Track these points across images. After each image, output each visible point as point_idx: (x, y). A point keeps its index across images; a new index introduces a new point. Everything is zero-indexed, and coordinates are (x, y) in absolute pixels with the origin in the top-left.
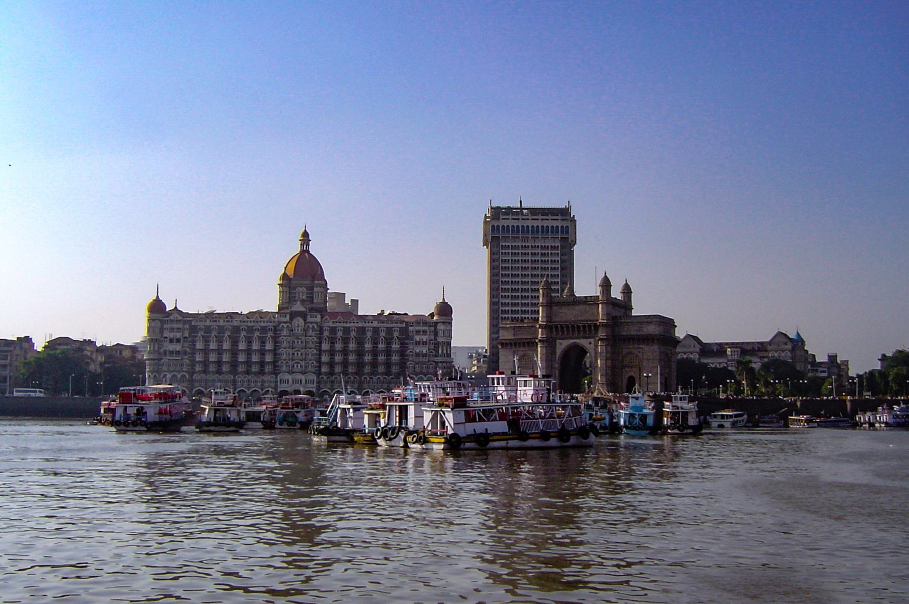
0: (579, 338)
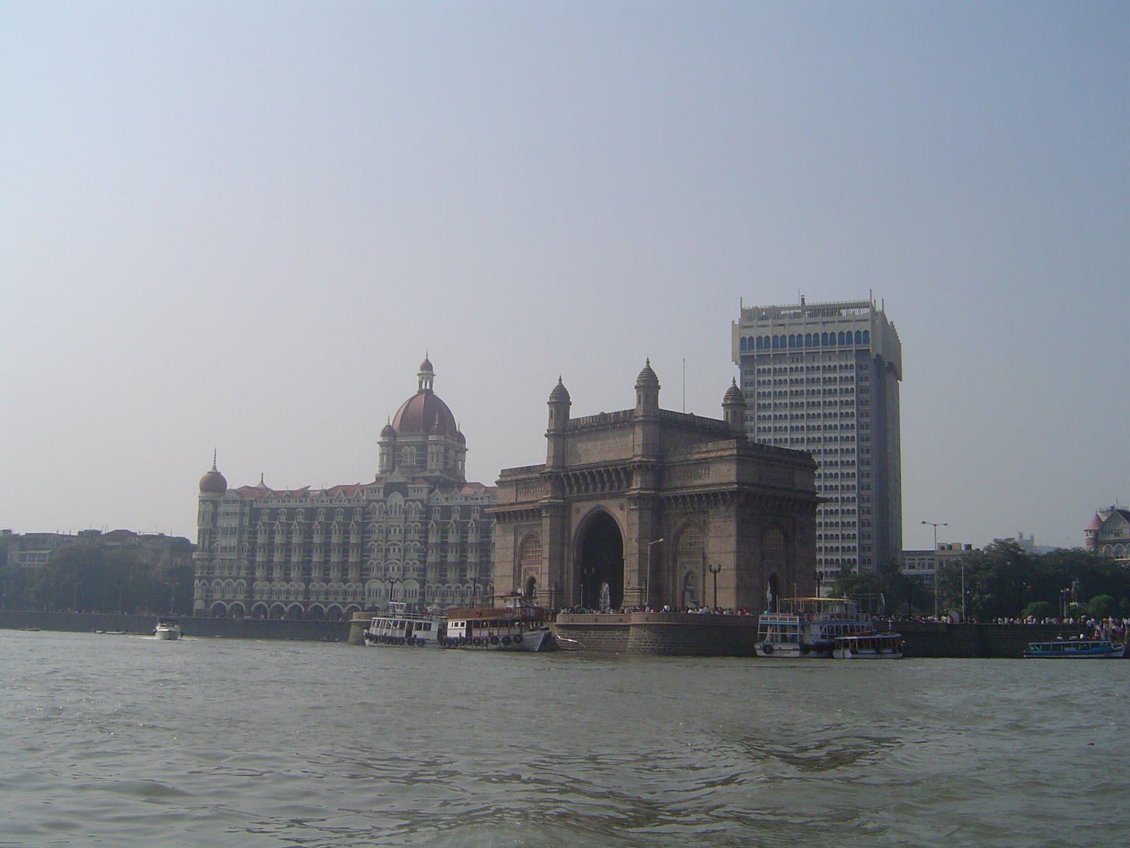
0: (604, 497)
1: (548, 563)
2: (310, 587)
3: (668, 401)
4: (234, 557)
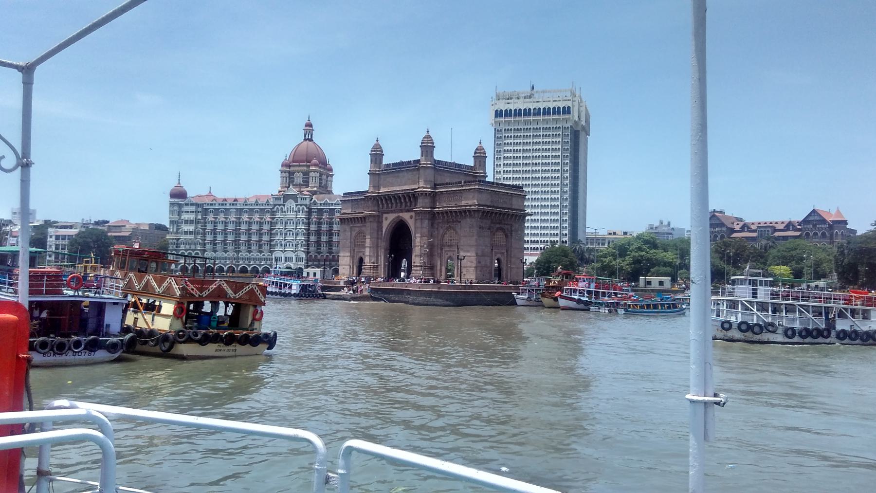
0: (402, 211)
1: (369, 249)
2: (239, 256)
3: (440, 154)
4: (192, 238)
